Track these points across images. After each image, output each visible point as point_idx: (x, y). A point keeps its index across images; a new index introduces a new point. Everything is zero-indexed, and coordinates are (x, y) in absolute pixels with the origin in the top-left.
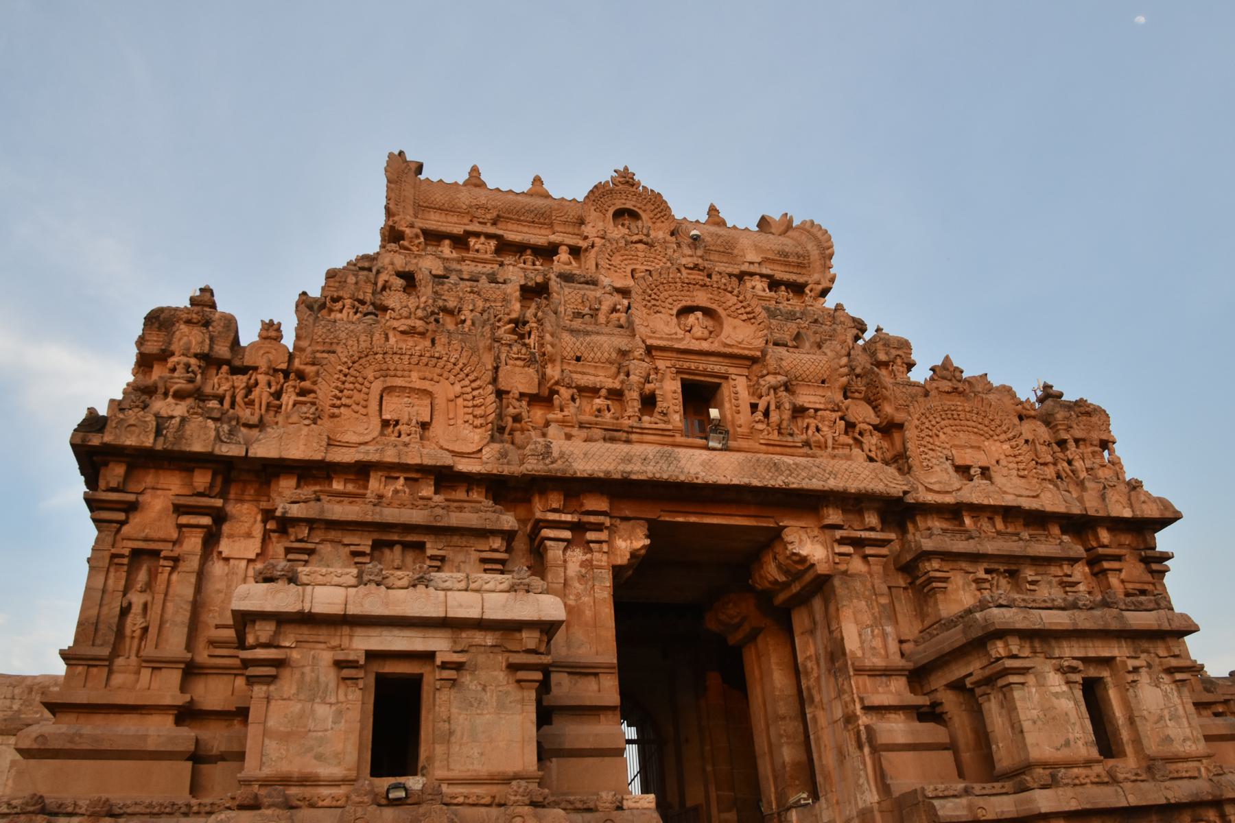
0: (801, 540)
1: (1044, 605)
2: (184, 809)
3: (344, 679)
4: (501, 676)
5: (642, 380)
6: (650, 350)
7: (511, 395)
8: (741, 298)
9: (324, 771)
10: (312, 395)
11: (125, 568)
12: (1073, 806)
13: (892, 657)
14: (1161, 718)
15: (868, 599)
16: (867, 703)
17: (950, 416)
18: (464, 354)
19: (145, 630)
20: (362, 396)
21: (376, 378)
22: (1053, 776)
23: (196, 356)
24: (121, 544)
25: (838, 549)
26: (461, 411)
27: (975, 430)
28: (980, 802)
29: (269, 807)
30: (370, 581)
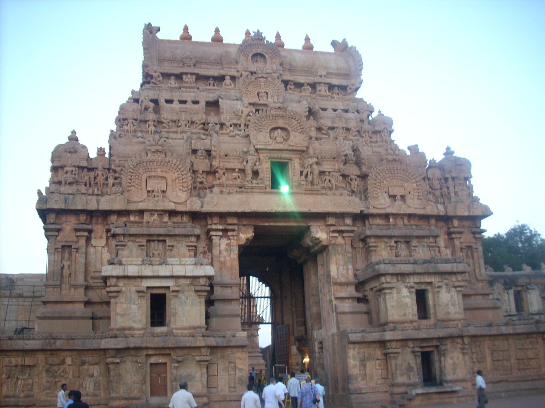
0: (317, 231)
1: (405, 262)
2: (93, 337)
3: (140, 296)
4: (193, 294)
6: (257, 150)
7: (199, 172)
8: (299, 121)
9: (135, 326)
10: (120, 179)
11: (60, 253)
12: (400, 337)
14: (448, 305)
16: (336, 296)
17: (390, 172)
19: (70, 274)
21: (144, 173)
22: (395, 327)
23: (74, 166)
25: (331, 235)
26: (178, 185)
27: (401, 178)
28: (367, 335)
29: (120, 337)
30: (146, 264)
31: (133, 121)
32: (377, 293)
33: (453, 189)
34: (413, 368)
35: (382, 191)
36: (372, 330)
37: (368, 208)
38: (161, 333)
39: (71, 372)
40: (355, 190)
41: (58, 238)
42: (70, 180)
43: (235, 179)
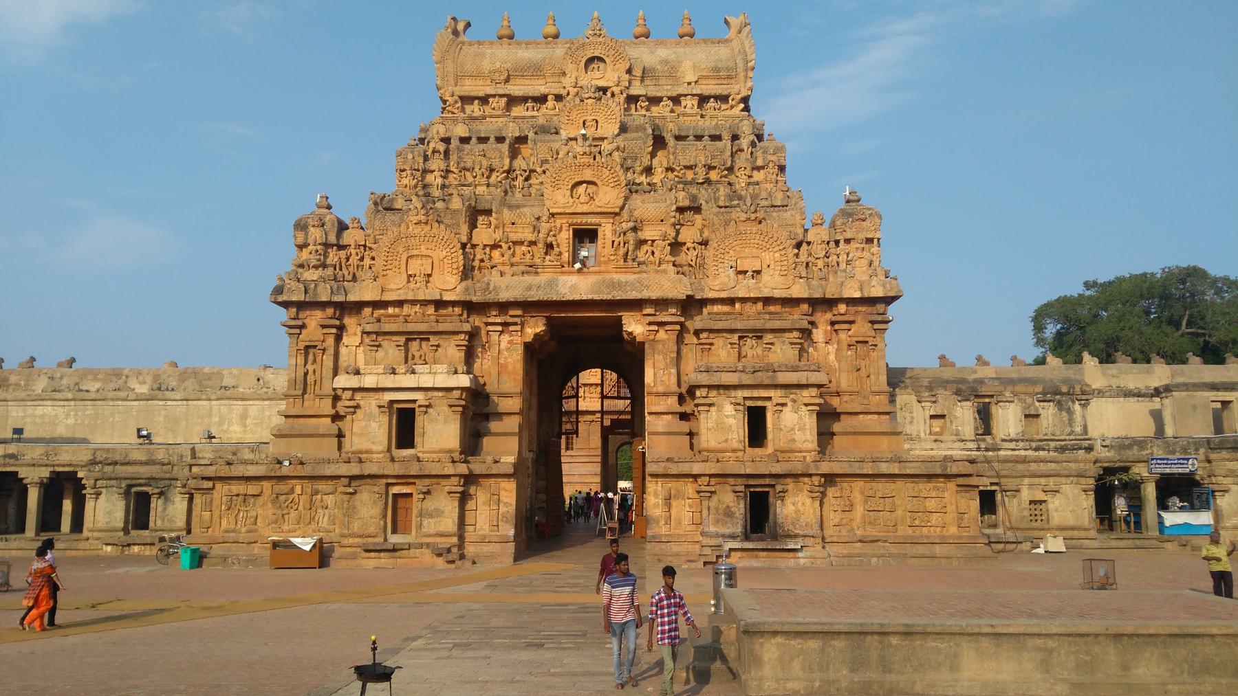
0: (630, 323)
4: (446, 409)
6: (553, 215)
9: (375, 448)
12: (713, 471)
14: (793, 429)
18: (447, 232)
20: (397, 263)
24: (300, 343)
26: (446, 266)
33: (845, 256)
35: (727, 265)
37: (702, 290)
39: (301, 503)
40: (693, 264)
42: (314, 262)
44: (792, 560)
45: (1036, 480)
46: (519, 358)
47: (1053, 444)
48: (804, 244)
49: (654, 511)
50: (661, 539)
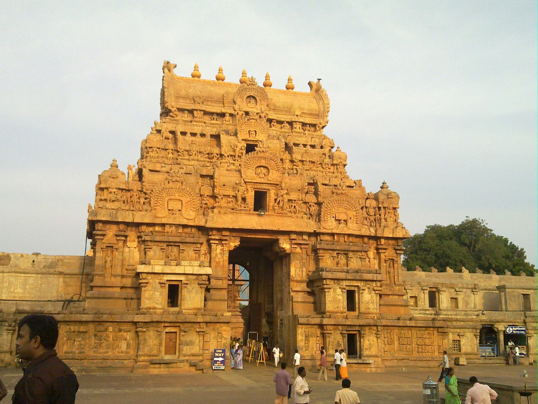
1: (340, 271)
4: (197, 286)
5: (242, 194)
6: (245, 182)
9: (157, 306)
12: (333, 323)
13: (303, 277)
14: (368, 302)
15: (300, 260)
23: (116, 188)
31: (157, 149)
32: (321, 290)
34: (341, 345)
35: (331, 216)
36: (315, 316)
37: (320, 228)
38: (175, 312)
40: (312, 213)
41: (104, 241)
42: (114, 199)
43: (229, 202)
44: (369, 369)
45: (456, 330)
46: (226, 258)
47: (463, 313)
48: (365, 209)
49: (300, 343)
50: (305, 357)
